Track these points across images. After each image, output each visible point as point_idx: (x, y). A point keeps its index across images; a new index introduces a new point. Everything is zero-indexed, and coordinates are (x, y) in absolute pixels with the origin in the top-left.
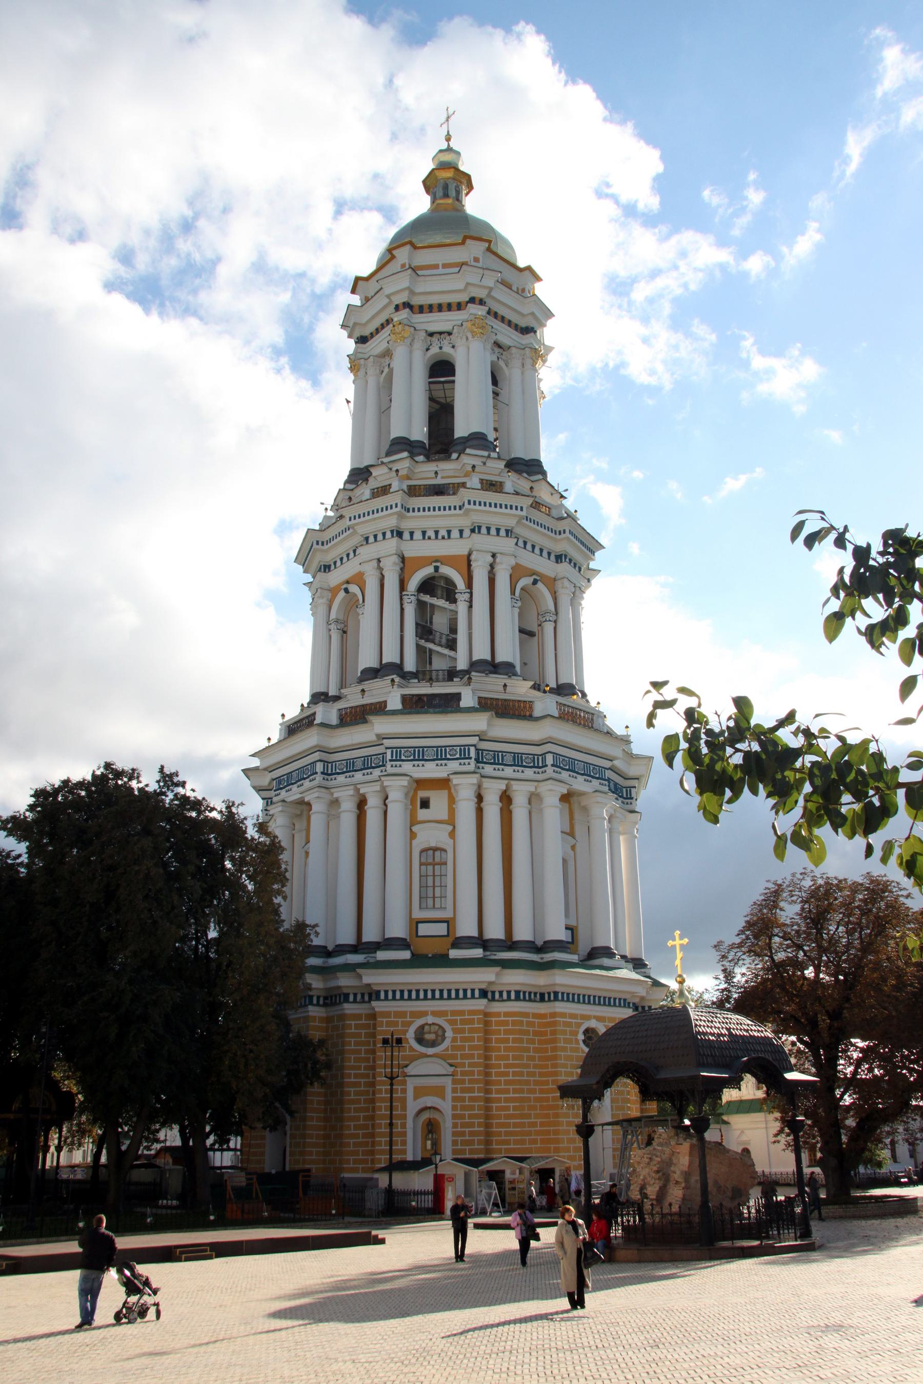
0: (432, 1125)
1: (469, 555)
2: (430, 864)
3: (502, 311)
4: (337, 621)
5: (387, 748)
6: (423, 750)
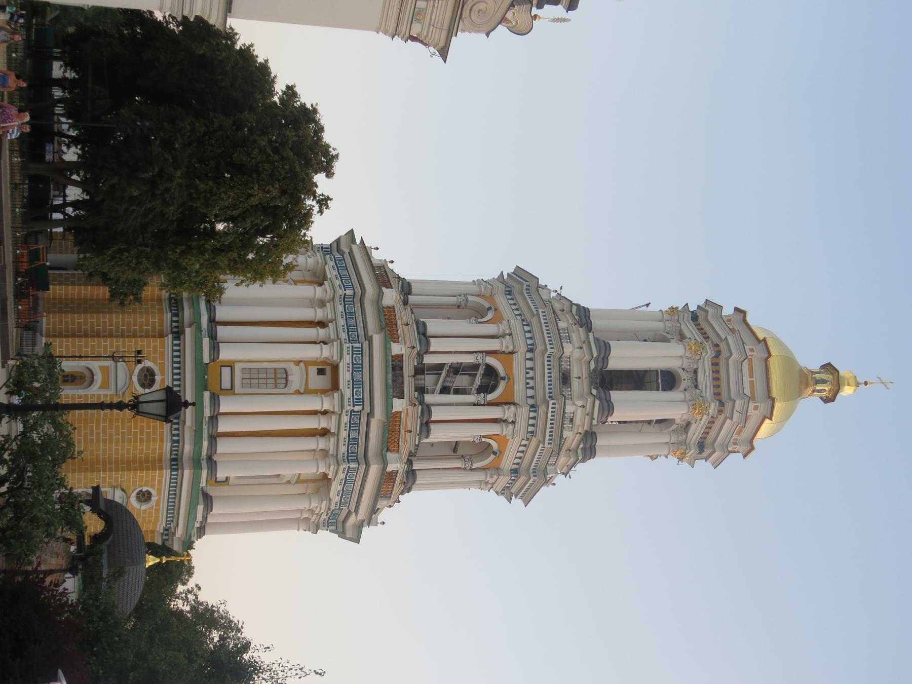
1: (514, 404)
2: (275, 375)
3: (716, 427)
4: (467, 300)
5: (362, 344)
6: (360, 371)
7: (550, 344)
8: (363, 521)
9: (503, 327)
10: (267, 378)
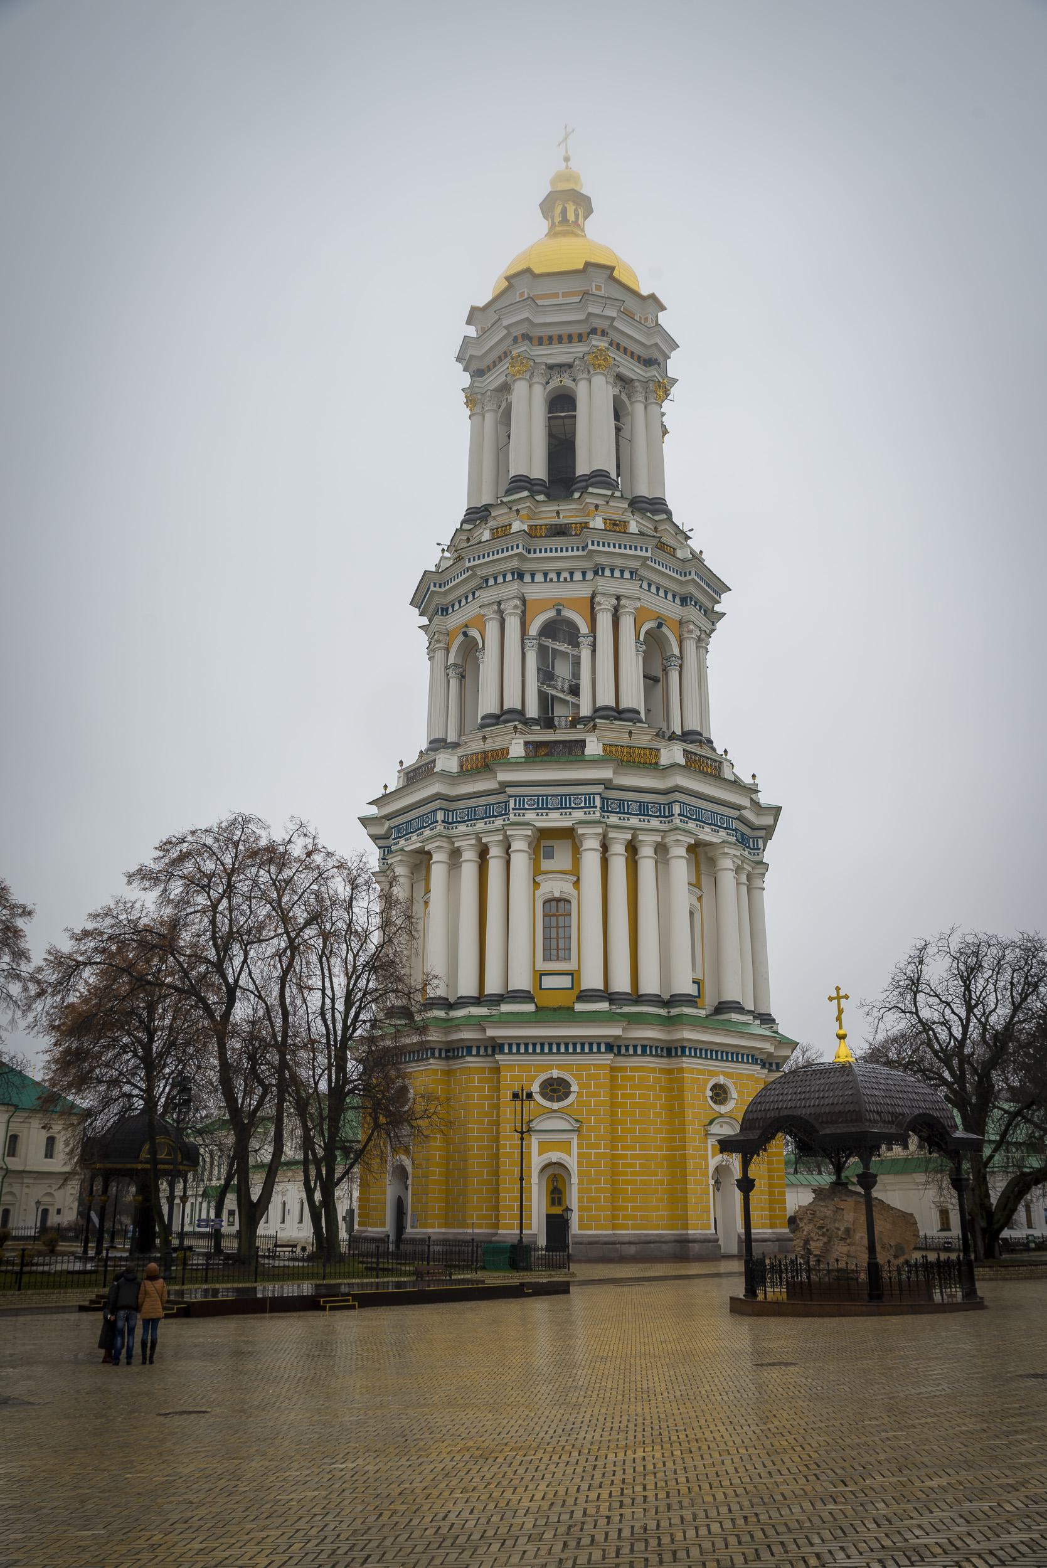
0: (557, 1181)
2: (553, 915)
3: (625, 342)
4: (455, 665)
5: (510, 797)
6: (547, 799)
7: (512, 549)
8: (752, 799)
9: (490, 613)
10: (558, 927)
